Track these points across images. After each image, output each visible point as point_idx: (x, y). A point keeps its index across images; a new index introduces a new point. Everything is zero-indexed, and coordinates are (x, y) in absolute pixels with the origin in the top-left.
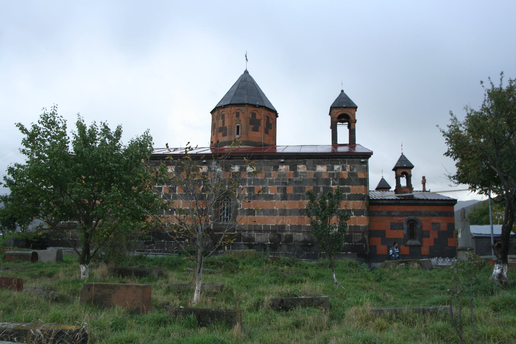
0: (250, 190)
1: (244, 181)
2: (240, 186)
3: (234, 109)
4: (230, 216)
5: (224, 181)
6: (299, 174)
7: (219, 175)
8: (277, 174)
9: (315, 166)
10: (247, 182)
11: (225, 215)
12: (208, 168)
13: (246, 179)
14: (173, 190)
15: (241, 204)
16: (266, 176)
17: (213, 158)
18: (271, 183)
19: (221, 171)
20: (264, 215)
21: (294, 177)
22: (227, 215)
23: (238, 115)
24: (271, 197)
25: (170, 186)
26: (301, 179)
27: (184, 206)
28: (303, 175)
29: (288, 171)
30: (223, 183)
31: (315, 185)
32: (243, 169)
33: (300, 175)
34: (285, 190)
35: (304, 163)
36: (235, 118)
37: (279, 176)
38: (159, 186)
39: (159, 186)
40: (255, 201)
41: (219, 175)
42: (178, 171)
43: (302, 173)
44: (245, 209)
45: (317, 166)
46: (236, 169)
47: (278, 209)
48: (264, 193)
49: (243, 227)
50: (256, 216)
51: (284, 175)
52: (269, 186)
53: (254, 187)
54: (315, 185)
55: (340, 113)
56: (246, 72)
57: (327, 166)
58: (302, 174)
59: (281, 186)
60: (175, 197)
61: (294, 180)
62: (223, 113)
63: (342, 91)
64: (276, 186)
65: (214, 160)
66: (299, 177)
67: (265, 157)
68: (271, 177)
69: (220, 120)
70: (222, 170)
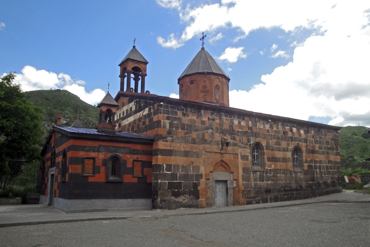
22: (257, 160)
56: (203, 49)
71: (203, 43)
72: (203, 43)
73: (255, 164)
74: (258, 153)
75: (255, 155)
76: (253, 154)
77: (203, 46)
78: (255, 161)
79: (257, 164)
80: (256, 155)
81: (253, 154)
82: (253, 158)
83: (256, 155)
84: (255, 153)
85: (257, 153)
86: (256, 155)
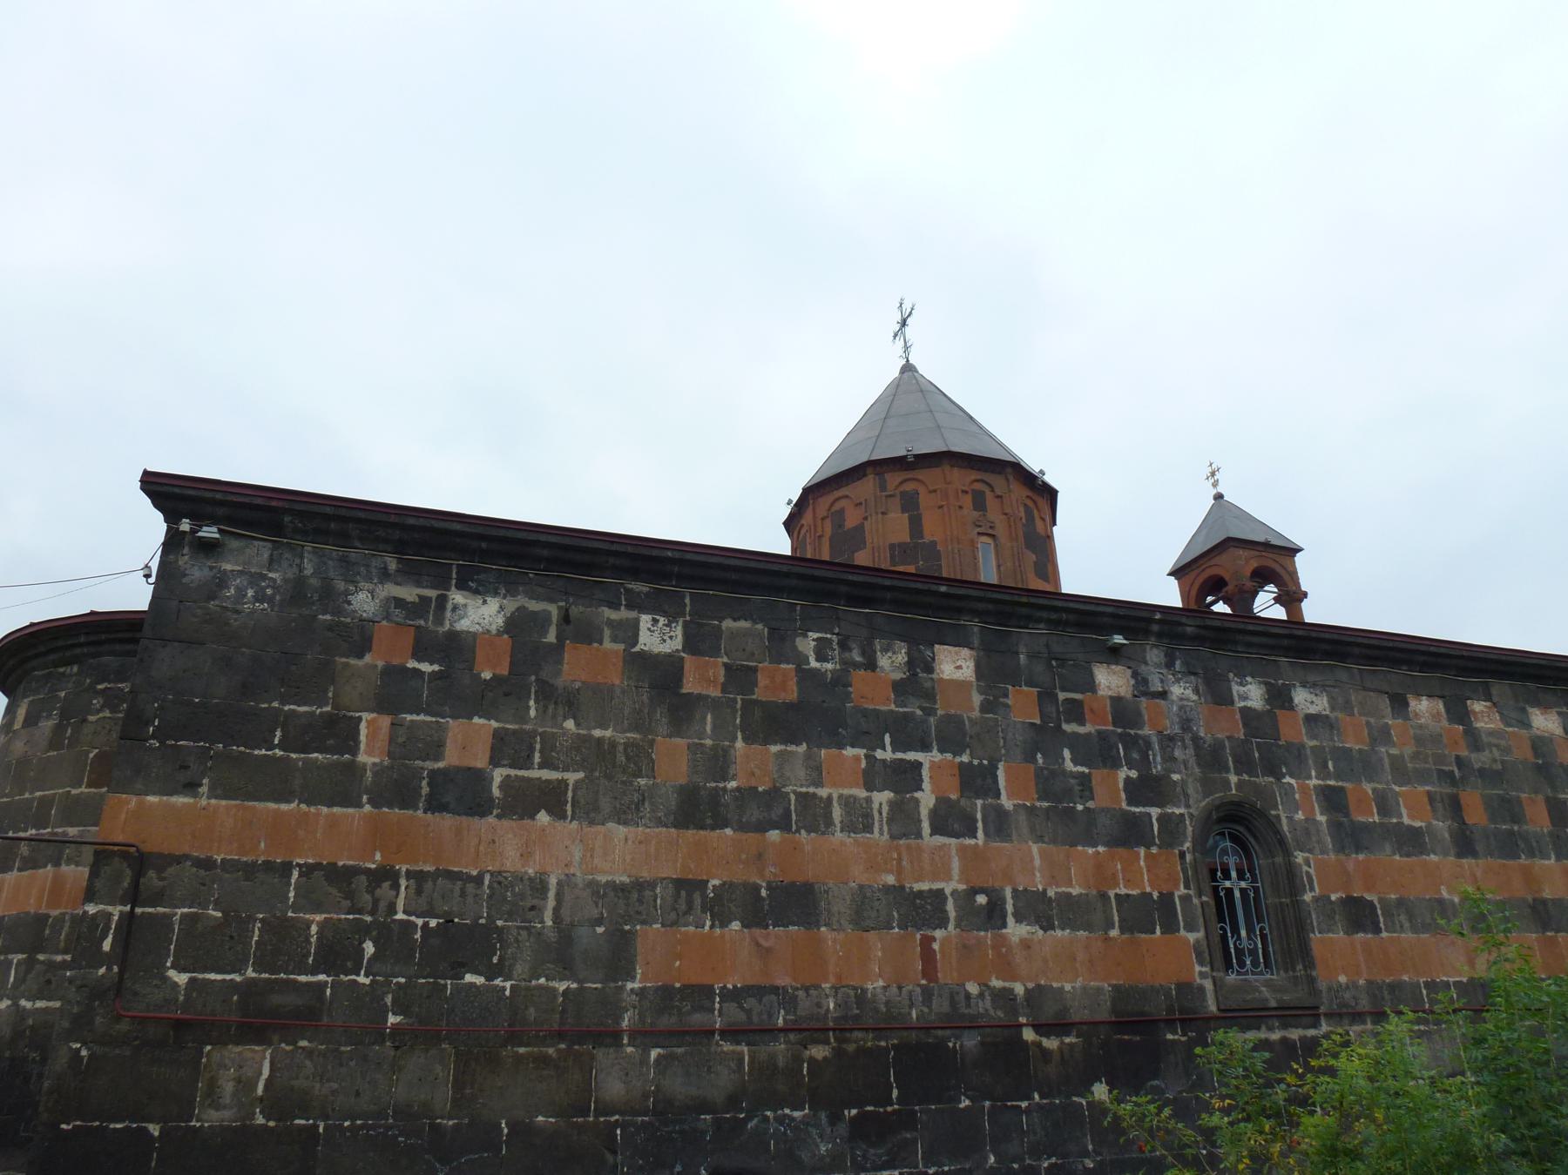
0: (1333, 800)
1: (1296, 758)
2: (1287, 779)
3: (960, 478)
4: (1263, 937)
5: (1217, 748)
6: (1485, 739)
7: (1189, 720)
8: (1412, 732)
9: (1523, 710)
10: (1310, 762)
11: (1243, 933)
12: (1135, 675)
13: (1303, 746)
14: (978, 781)
15: (1312, 871)
16: (1374, 741)
17: (1155, 628)
18: (1401, 773)
19: (1195, 698)
20: (1415, 930)
21: (1472, 752)
22: (1250, 930)
23: (979, 503)
24: (1412, 841)
25: (965, 758)
26: (1495, 761)
27: (1053, 880)
28: (1497, 746)
29: (1445, 723)
30: (1211, 758)
31: (1549, 792)
32: (1279, 698)
33: (1490, 745)
34: (1455, 807)
35: (1488, 698)
36: (970, 513)
37: (1419, 741)
38: (900, 755)
39: (900, 755)
40: (1361, 857)
41: (1189, 720)
42: (994, 674)
43: (1491, 733)
44: (1333, 897)
45: (1530, 710)
46: (1252, 694)
47: (1456, 900)
48: (1386, 820)
49: (1347, 995)
50: (1384, 934)
51: (1436, 739)
52: (1397, 789)
53: (1342, 789)
54: (1549, 792)
55: (1254, 564)
56: (908, 368)
57: (1559, 714)
58: (1494, 741)
59: (1438, 789)
60: (1000, 824)
61: (1476, 766)
62: (909, 487)
63: (1219, 497)
64: (1420, 789)
65: (1153, 640)
66: (1487, 752)
67: (1356, 650)
68: (1394, 745)
69: (891, 515)
70: (1196, 691)
71: (906, 348)
72: (906, 348)
73: (1239, 952)
74: (1254, 880)
75: (1229, 891)
76: (1215, 890)
77: (908, 361)
78: (1239, 937)
79: (1253, 952)
80: (1237, 894)
81: (1215, 890)
82: (1221, 919)
83: (1237, 894)
84: (1227, 876)
85: (1241, 877)
86: (1243, 891)
